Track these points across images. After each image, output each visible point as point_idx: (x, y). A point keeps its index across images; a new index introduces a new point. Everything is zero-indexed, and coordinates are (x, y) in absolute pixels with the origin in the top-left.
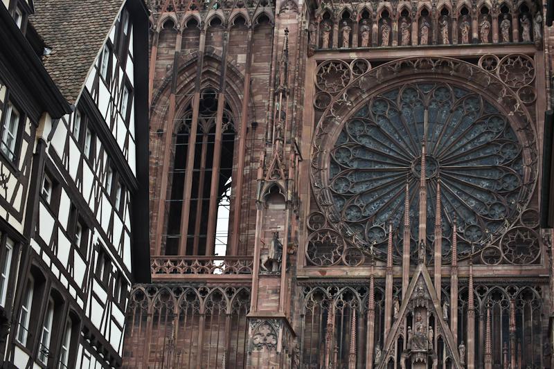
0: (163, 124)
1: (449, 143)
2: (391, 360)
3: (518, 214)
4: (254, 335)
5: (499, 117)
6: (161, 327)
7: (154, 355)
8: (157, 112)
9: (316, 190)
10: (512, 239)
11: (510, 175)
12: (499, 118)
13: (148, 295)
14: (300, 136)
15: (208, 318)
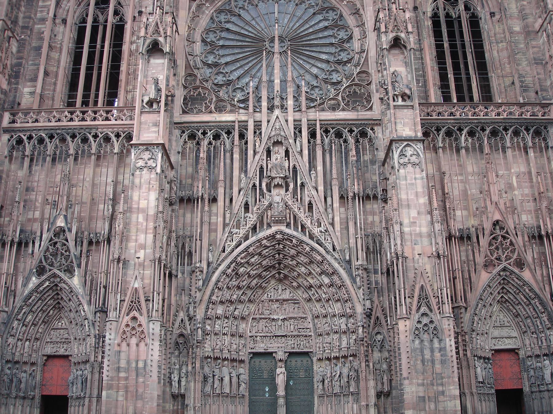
0: (67, 15)
1: (295, 27)
2: (254, 185)
3: (353, 74)
4: (136, 159)
5: (333, 9)
6: (59, 167)
7: (51, 189)
8: (62, 6)
9: (190, 58)
10: (349, 92)
11: (343, 50)
12: (334, 11)
13: (47, 140)
14: (177, 15)
15: (98, 158)
